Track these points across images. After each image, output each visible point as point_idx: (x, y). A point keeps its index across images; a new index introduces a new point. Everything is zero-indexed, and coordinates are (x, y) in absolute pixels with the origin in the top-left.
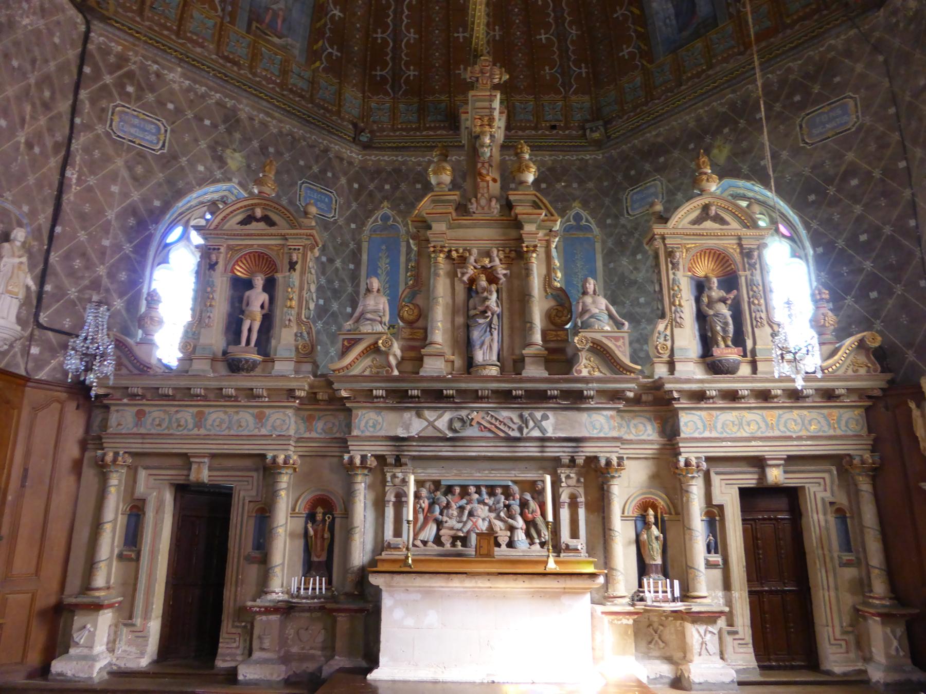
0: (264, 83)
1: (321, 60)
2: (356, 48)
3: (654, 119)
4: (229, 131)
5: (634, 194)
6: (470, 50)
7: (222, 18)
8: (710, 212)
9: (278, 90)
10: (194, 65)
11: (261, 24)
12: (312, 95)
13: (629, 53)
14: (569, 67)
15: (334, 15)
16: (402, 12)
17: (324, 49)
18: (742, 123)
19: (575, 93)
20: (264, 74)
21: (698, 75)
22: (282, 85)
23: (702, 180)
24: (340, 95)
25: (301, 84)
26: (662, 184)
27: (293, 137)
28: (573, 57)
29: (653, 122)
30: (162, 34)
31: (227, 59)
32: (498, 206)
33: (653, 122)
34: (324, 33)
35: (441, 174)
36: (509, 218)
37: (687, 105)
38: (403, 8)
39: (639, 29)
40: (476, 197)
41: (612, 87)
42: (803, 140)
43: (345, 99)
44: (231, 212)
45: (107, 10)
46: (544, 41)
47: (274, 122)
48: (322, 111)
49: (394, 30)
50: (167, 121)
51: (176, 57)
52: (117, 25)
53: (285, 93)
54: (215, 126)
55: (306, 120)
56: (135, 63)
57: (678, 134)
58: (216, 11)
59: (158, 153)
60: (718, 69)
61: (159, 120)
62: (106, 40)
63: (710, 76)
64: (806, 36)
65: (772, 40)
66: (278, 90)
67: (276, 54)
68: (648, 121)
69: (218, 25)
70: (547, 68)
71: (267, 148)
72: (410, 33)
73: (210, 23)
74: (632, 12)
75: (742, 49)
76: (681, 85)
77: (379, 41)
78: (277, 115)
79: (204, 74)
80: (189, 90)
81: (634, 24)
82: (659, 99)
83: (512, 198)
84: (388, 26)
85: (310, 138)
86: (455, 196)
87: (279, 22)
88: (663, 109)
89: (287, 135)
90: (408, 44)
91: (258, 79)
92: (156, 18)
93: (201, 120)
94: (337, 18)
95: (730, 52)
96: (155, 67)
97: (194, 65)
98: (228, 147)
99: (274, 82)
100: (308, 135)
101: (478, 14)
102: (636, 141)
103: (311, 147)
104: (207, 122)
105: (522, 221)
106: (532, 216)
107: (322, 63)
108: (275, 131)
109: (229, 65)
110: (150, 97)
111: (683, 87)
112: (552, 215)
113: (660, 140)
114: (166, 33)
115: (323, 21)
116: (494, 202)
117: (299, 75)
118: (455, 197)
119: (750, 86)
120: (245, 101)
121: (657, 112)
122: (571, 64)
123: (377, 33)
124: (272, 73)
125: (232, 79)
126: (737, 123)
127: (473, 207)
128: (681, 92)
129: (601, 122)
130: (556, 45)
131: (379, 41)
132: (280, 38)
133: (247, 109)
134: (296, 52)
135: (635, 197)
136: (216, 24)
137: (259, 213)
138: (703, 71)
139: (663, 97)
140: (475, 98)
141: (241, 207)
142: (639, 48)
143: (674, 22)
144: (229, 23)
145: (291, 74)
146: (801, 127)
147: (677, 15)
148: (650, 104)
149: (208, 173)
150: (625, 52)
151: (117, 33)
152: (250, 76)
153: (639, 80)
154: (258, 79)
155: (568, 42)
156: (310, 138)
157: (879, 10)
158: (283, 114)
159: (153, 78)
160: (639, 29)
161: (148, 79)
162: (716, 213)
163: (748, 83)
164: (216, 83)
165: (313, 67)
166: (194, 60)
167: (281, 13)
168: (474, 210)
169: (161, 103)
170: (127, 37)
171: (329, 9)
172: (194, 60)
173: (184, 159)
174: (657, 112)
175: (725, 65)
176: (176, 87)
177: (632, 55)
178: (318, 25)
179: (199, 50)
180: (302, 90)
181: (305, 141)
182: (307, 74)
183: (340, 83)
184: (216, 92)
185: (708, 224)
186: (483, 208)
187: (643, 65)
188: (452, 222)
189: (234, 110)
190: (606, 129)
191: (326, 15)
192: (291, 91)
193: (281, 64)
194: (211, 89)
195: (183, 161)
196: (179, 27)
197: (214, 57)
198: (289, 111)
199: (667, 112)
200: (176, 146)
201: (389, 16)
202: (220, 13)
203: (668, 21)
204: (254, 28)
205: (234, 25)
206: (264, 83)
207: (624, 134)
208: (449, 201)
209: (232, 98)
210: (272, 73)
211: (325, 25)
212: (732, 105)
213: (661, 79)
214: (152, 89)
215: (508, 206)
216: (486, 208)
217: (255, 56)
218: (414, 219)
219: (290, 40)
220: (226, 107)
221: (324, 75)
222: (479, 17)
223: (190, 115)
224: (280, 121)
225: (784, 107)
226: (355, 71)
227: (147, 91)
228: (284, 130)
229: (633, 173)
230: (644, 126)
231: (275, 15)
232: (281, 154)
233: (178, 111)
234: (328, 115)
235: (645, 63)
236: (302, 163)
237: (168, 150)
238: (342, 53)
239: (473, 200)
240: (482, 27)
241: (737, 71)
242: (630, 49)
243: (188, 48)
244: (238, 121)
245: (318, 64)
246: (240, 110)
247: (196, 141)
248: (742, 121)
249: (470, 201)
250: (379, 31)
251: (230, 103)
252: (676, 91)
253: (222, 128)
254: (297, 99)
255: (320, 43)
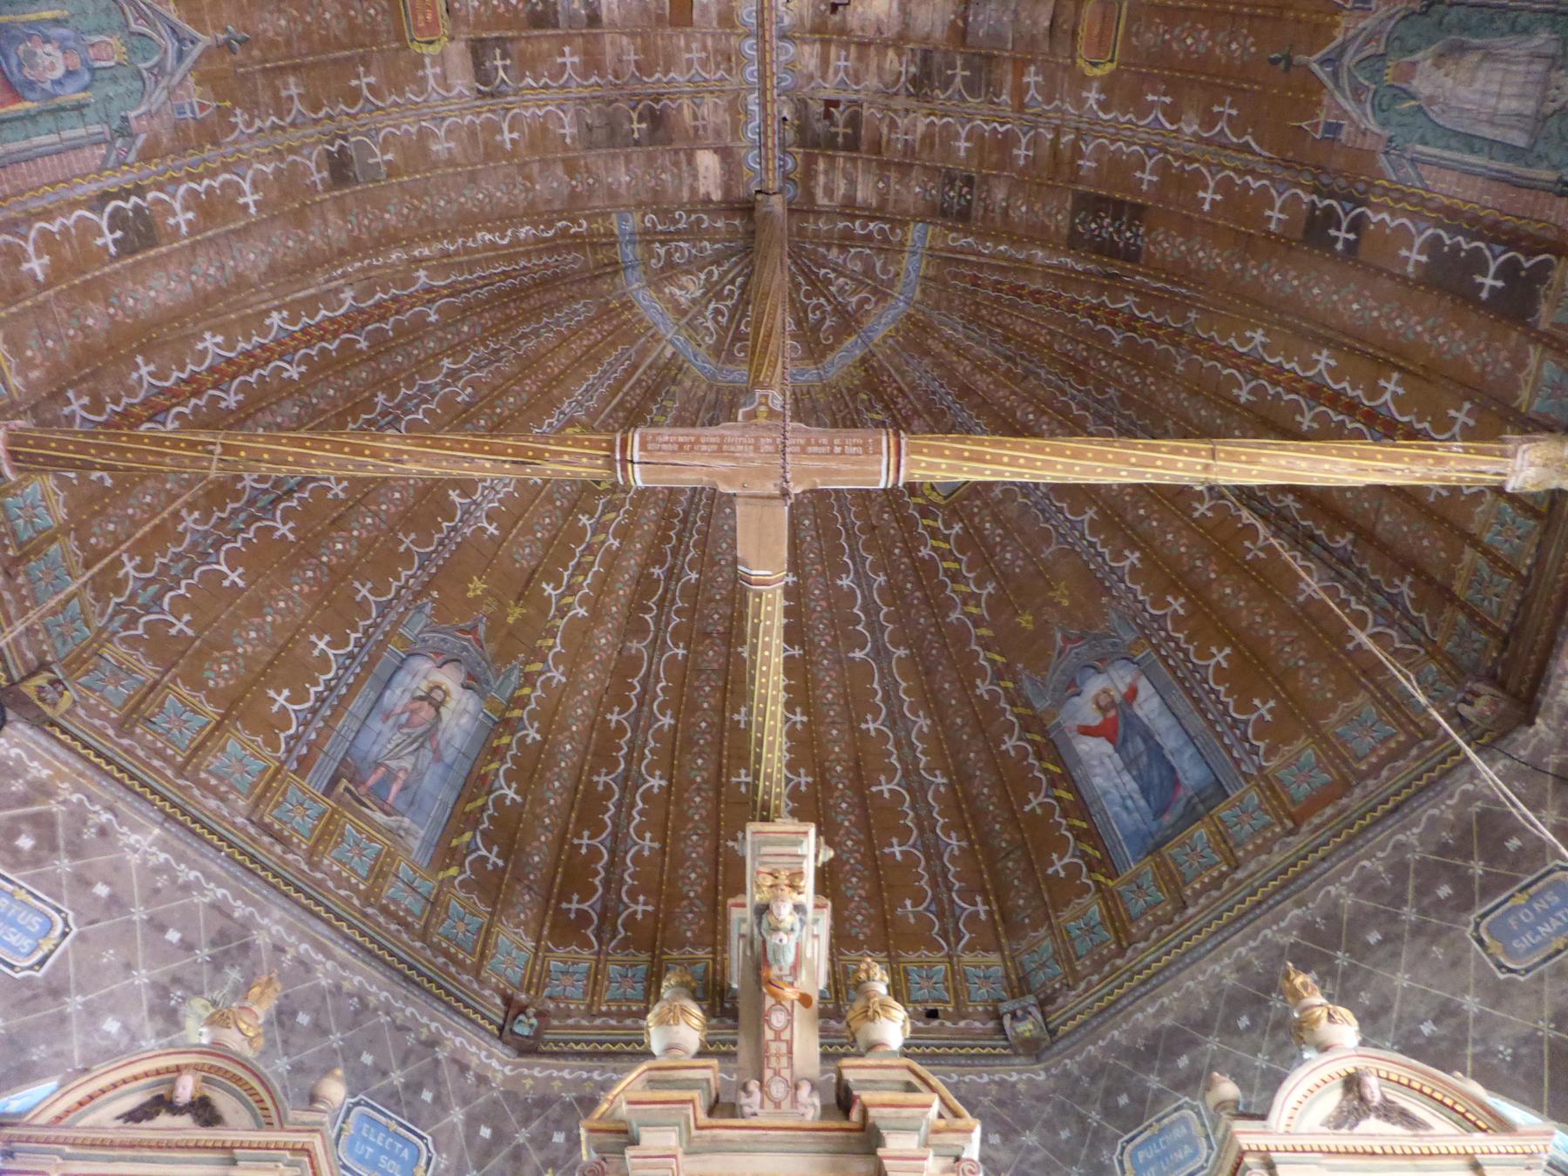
0: (330, 884)
1: (462, 865)
2: (537, 859)
3: (1143, 983)
4: (217, 964)
5: (1138, 1147)
6: (755, 802)
7: (283, 763)
8: (1367, 1093)
9: (356, 902)
10: (193, 832)
11: (357, 787)
12: (426, 927)
13: (1065, 867)
14: (952, 901)
15: (505, 796)
16: (633, 805)
17: (470, 848)
18: (1342, 959)
19: (970, 947)
20: (335, 868)
21: (1216, 883)
22: (366, 898)
23: (1318, 1020)
24: (488, 932)
25: (408, 901)
26: (1199, 1114)
27: (364, 1005)
28: (957, 885)
29: (1143, 990)
30: (149, 766)
31: (267, 829)
32: (817, 1101)
33: (1143, 990)
34: (478, 822)
35: (677, 1024)
36: (846, 1125)
37: (1209, 946)
38: (634, 797)
39: (1077, 823)
40: (761, 1080)
41: (1043, 931)
42: (1500, 966)
43: (496, 944)
44: (115, 1086)
45: (54, 705)
46: (899, 857)
47: (330, 964)
48: (441, 960)
49: (614, 835)
50: (78, 914)
51: (162, 810)
52: (62, 737)
53: (370, 911)
54: (188, 946)
55: (408, 975)
56: (65, 802)
57: (1205, 1004)
58: (276, 749)
59: (17, 976)
60: (1252, 866)
61: (59, 911)
62: (24, 755)
63: (1240, 882)
64: (1408, 786)
65: (1344, 801)
66: (356, 902)
67: (371, 839)
68: (1133, 989)
69: (271, 771)
70: (908, 903)
71: (294, 1014)
72: (643, 839)
73: (257, 765)
74: (1059, 799)
75: (1289, 824)
76: (1185, 907)
77: (584, 851)
78: (339, 952)
79: (207, 849)
80: (164, 869)
81: (1065, 816)
82: (1146, 939)
83: (850, 1076)
84: (604, 826)
85: (402, 1010)
86: (710, 1072)
87: (395, 788)
88: (1158, 960)
89: (351, 995)
90: (637, 859)
91: (319, 875)
92: (149, 737)
93: (162, 929)
94: (508, 802)
95: (1269, 835)
96: (105, 817)
97: (193, 832)
98: (200, 993)
99: (354, 889)
100: (399, 1004)
101: (769, 723)
102: (1116, 1033)
103: (402, 1029)
104: (173, 936)
105: (880, 1123)
106: (906, 1112)
107: (461, 872)
108: (324, 982)
109: (266, 839)
110: (64, 865)
111: (1191, 911)
112: (957, 1115)
113: (1168, 1021)
114: (156, 763)
115: (480, 802)
116: (805, 1090)
117: (409, 885)
118: (708, 1074)
119: (1332, 889)
120: (277, 913)
121: (1148, 967)
122: (954, 895)
123: (581, 838)
124: (353, 870)
125: (265, 868)
126: (1330, 959)
127: (752, 1101)
128: (1190, 918)
129: (1031, 999)
130: (923, 863)
131: (584, 851)
132: (387, 814)
133: (275, 929)
134: (415, 844)
135: (1141, 1155)
136: (267, 768)
137: (186, 1089)
138: (1223, 875)
139: (1154, 935)
140: (759, 837)
141: (146, 1075)
142: (1084, 855)
143: (1142, 803)
144: (295, 772)
145: (392, 879)
146: (1481, 942)
147: (1145, 791)
148: (1129, 953)
149: (125, 1040)
150: (1058, 866)
151: (57, 749)
152: (305, 868)
153: (1096, 911)
154: (319, 875)
155: (945, 859)
156: (402, 1010)
157: (1531, 723)
158: (355, 955)
159: (89, 834)
160: (1077, 823)
161: (79, 833)
162: (1383, 1096)
163: (1328, 882)
164: (227, 871)
165: (441, 875)
166: (194, 821)
167: (401, 775)
168: (756, 1109)
169: (83, 882)
170: (72, 759)
171: (496, 785)
172: (194, 821)
173: (79, 999)
174: (1148, 967)
175: (1264, 857)
176: (134, 859)
177: (1073, 871)
178: (469, 807)
179: (212, 803)
180: (408, 911)
181: (388, 1014)
182: (428, 886)
183: (492, 914)
184: (220, 885)
185: (1372, 1124)
186: (777, 1105)
187: (1097, 883)
188: (694, 1133)
189: (246, 926)
190: (1043, 1014)
191: (490, 792)
192: (384, 910)
193: (376, 859)
194: (209, 877)
195: (74, 1003)
196: (188, 761)
197: (240, 820)
198: (369, 952)
199: (1168, 965)
200: (72, 969)
201: (608, 810)
202: (282, 754)
203: (1129, 803)
204: (341, 788)
205: (303, 778)
206: (330, 884)
207: (1083, 1024)
208: (690, 1085)
209: (249, 901)
210: (353, 870)
211: (483, 808)
212: (1307, 929)
213: (1141, 902)
214: (76, 851)
215: (843, 1100)
216: (786, 1105)
217: (327, 834)
218: (596, 1125)
219: (407, 822)
220: (229, 917)
221: (462, 894)
222: (772, 731)
223: (139, 914)
224: (344, 966)
225: (1423, 911)
226: (527, 898)
227: (62, 854)
228: (346, 985)
229: (1123, 1100)
230: (1125, 1002)
231: (391, 776)
232: (326, 1033)
233: (115, 903)
234: (453, 970)
235: (1102, 879)
236: (367, 1059)
237: (46, 976)
238: (506, 861)
239: (753, 1086)
240: (777, 754)
241: (1295, 865)
242: (1066, 860)
243: (192, 797)
244: (245, 948)
245: (453, 871)
246: (259, 927)
247: (128, 967)
248: (1339, 954)
249: (744, 1088)
250: (586, 833)
251: (240, 910)
252: (1177, 919)
253: (203, 953)
254: (393, 927)
255: (467, 836)
